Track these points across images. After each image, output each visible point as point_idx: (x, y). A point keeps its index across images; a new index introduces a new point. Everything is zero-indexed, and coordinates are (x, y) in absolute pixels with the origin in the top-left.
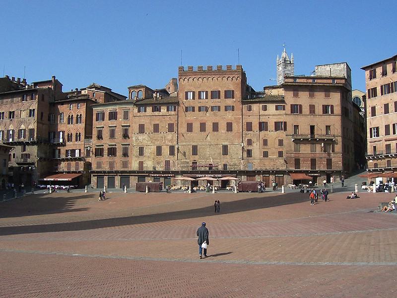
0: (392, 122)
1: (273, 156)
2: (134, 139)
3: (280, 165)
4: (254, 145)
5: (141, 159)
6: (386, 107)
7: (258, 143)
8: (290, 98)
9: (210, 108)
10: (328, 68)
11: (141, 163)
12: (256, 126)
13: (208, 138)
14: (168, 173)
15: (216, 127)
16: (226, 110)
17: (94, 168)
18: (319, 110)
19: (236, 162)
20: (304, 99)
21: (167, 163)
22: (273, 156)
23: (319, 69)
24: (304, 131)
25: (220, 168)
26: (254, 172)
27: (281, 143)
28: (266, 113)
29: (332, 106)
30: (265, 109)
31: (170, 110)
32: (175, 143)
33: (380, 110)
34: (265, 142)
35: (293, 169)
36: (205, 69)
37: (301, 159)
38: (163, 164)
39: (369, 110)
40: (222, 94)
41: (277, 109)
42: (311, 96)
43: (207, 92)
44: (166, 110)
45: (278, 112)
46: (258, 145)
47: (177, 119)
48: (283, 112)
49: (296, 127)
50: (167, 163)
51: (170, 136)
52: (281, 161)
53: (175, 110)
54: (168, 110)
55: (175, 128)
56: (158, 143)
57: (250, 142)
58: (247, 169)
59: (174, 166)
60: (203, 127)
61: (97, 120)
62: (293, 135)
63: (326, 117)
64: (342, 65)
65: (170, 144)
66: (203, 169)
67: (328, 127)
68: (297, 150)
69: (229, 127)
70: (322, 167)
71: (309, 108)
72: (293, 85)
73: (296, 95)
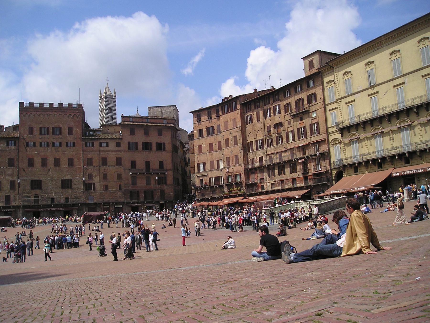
0: (216, 158)
3: (120, 197)
4: (95, 179)
6: (211, 145)
7: (98, 177)
8: (128, 138)
9: (52, 144)
10: (160, 109)
12: (96, 162)
13: (50, 173)
14: (9, 207)
15: (57, 162)
16: (67, 145)
19: (78, 195)
21: (8, 198)
22: (113, 189)
24: (141, 165)
25: (63, 201)
26: (95, 204)
27: (119, 176)
29: (164, 144)
31: (10, 144)
32: (15, 177)
33: (205, 148)
34: (105, 177)
36: (46, 105)
39: (196, 148)
42: (147, 133)
43: (48, 128)
44: (6, 144)
45: (117, 149)
46: (99, 179)
47: (17, 154)
49: (133, 163)
50: (8, 198)
51: (10, 171)
52: (120, 194)
53: (15, 145)
54: (8, 145)
55: (16, 163)
57: (91, 176)
58: (88, 202)
59: (15, 200)
60: (44, 163)
64: (172, 108)
65: (11, 179)
66: (45, 203)
67: (161, 164)
68: (134, 182)
69: (71, 162)
73: (132, 133)
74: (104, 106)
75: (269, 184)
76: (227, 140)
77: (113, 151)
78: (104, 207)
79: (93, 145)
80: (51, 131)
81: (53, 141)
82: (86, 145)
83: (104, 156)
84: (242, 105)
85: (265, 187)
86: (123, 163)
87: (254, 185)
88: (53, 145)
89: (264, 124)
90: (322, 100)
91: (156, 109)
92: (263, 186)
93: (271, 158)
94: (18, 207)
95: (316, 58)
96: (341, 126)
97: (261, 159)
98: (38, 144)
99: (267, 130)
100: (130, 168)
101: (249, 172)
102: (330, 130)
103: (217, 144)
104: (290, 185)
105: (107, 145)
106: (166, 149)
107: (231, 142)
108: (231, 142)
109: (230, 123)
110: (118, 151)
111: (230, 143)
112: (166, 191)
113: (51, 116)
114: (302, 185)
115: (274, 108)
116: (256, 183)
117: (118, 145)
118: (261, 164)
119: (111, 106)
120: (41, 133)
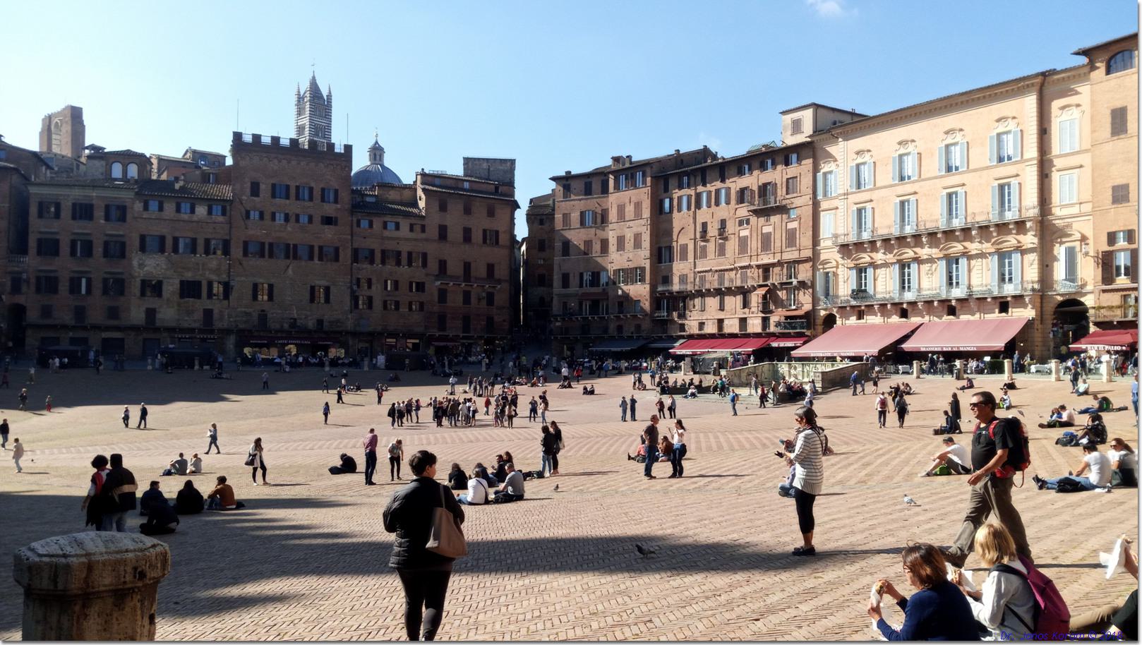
2: (135, 263)
4: (374, 287)
5: (151, 302)
11: (151, 313)
13: (290, 271)
17: (33, 316)
18: (477, 236)
20: (455, 220)
21: (208, 314)
24: (455, 268)
25: (311, 324)
29: (497, 232)
38: (199, 315)
40: (317, 194)
41: (411, 230)
42: (467, 211)
48: (423, 236)
50: (208, 314)
52: (416, 318)
53: (224, 214)
54: (210, 212)
56: (189, 276)
61: (40, 215)
63: (486, 249)
66: (278, 326)
67: (491, 268)
74: (305, 121)
76: (621, 241)
79: (371, 225)
80: (293, 192)
81: (297, 211)
82: (358, 225)
84: (655, 178)
88: (297, 220)
93: (703, 279)
94: (228, 332)
95: (807, 116)
96: (841, 240)
98: (267, 216)
99: (699, 229)
105: (397, 227)
106: (501, 242)
108: (629, 244)
109: (630, 210)
112: (496, 319)
113: (294, 163)
115: (718, 191)
119: (323, 122)
120: (274, 196)
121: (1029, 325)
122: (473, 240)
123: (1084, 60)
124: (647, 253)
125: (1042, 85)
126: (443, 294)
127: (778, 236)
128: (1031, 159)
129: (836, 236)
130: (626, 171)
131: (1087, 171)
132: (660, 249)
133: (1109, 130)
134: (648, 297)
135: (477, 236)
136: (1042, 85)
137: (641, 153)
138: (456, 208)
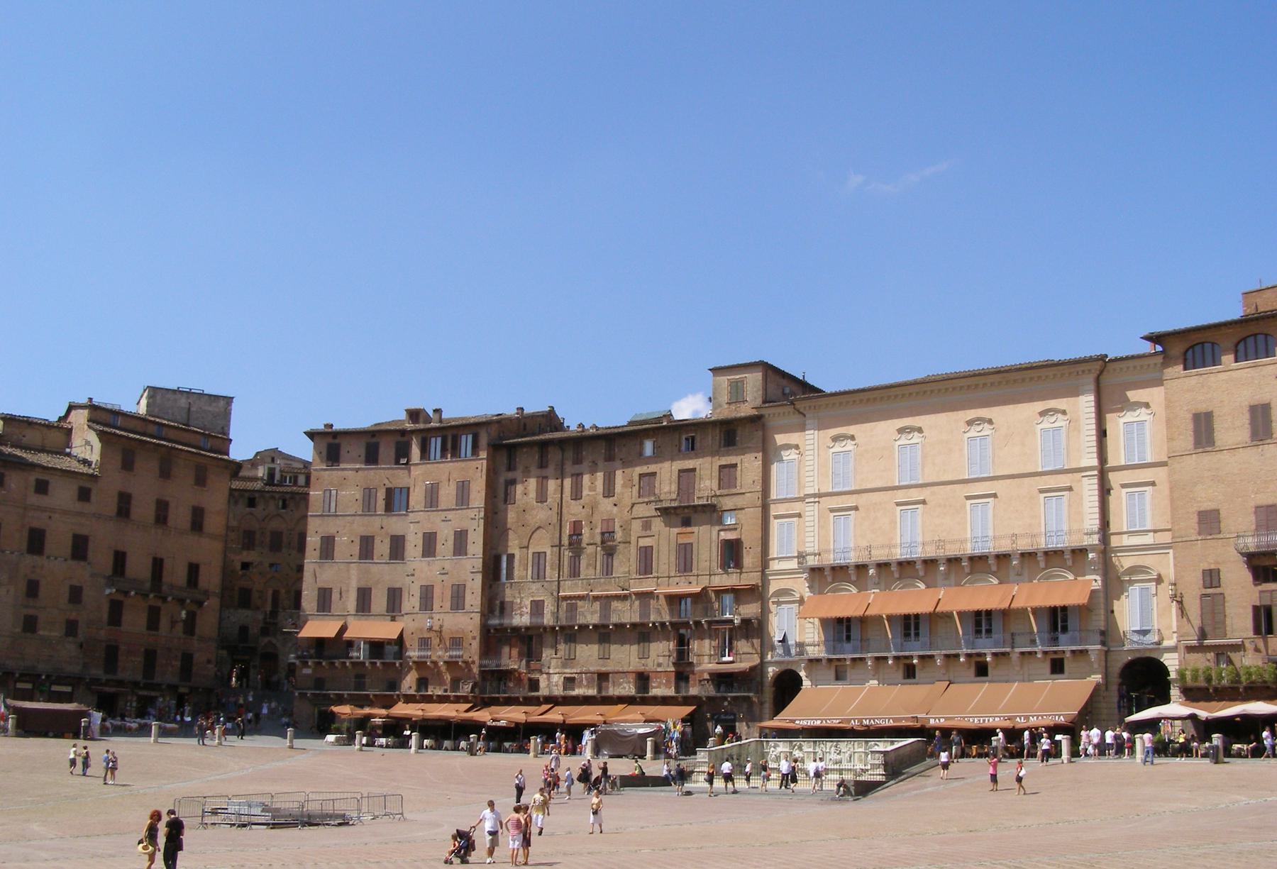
1: (51, 631)
23: (158, 397)
24: (138, 567)
27: (76, 595)
28: (43, 501)
30: (42, 488)
33: (346, 545)
34: (33, 589)
35: (98, 672)
37: (123, 647)
39: (313, 541)
42: (165, 473)
45: (79, 506)
49: (120, 559)
62: (109, 578)
67: (194, 570)
70: (168, 673)
71: (153, 507)
72: (127, 438)
75: (555, 678)
77: (65, 512)
78: (20, 685)
83: (36, 524)
85: (543, 684)
86: (90, 554)
87: (503, 676)
89: (560, 514)
90: (759, 488)
91: (170, 396)
92: (534, 685)
93: (572, 609)
95: (753, 381)
96: (812, 561)
97: (537, 607)
99: (567, 530)
100: (109, 572)
101: (493, 638)
102: (775, 566)
103: (387, 541)
104: (629, 689)
107: (445, 545)
108: (445, 545)
109: (448, 494)
110: (80, 514)
111: (439, 547)
112: (196, 656)
114: (670, 692)
116: (515, 670)
117: (84, 495)
118: (534, 620)
121: (1097, 688)
122: (171, 522)
123: (1147, 347)
124: (479, 564)
125: (1101, 372)
126: (116, 609)
127: (664, 549)
128: (1091, 468)
129: (801, 556)
130: (447, 437)
131: (1164, 487)
132: (497, 560)
133: (1191, 439)
134: (477, 633)
135: (180, 516)
136: (1101, 372)
137: (459, 408)
138: (147, 468)
